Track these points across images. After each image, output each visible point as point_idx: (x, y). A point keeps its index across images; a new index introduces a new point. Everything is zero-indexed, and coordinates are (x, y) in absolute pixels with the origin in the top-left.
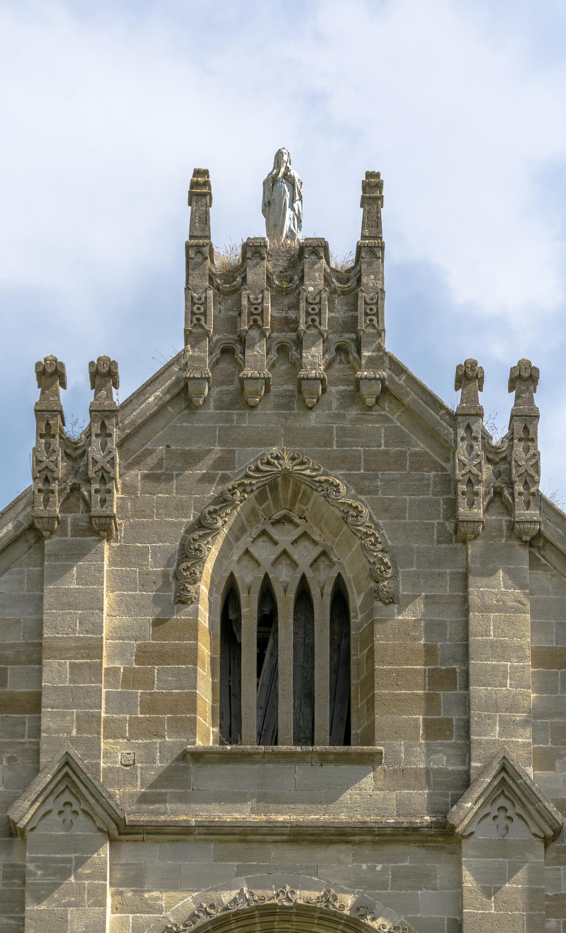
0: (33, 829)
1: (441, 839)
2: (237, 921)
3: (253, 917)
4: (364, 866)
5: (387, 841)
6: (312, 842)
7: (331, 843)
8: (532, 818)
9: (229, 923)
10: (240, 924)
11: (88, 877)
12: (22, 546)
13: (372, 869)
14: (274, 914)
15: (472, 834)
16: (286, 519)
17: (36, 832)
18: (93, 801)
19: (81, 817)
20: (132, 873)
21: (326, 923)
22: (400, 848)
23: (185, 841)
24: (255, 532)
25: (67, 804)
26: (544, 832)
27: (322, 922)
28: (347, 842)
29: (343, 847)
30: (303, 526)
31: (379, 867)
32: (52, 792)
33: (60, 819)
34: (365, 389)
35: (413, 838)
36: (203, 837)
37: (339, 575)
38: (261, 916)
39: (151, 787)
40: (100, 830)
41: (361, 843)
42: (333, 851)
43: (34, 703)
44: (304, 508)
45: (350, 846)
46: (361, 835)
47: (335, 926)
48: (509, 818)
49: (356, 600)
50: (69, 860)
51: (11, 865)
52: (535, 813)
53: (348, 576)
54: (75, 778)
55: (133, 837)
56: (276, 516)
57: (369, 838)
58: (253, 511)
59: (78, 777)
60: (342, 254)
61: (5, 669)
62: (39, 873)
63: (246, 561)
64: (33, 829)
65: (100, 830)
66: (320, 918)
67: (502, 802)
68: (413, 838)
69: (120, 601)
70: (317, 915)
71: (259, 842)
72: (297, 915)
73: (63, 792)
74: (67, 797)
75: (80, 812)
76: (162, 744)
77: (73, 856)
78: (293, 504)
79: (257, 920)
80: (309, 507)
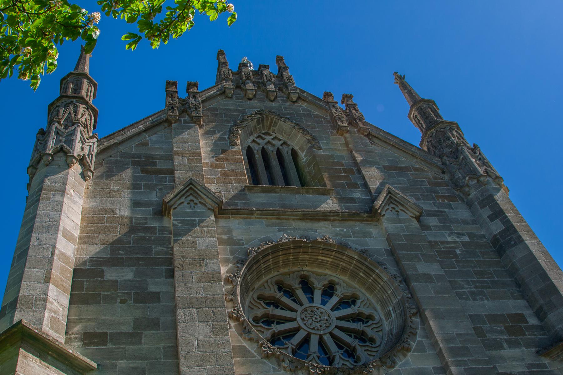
0: (175, 208)
1: (370, 219)
2: (283, 250)
3: (289, 249)
4: (338, 229)
5: (345, 220)
6: (311, 220)
7: (319, 220)
8: (408, 210)
9: (278, 251)
10: (284, 252)
11: (205, 227)
12: (161, 127)
13: (343, 230)
14: (300, 247)
15: (384, 215)
16: (267, 134)
17: (177, 210)
18: (204, 197)
19: (199, 205)
20: (226, 230)
21: (326, 252)
22: (352, 223)
23: (250, 218)
24: (256, 135)
25: (191, 201)
26: (415, 215)
27: (324, 252)
28: (327, 220)
29: (326, 222)
30: (274, 135)
31: (345, 230)
32: (183, 195)
33: (189, 206)
34: (292, 96)
35: (357, 218)
36: (259, 216)
37: (293, 149)
38: (295, 248)
39: (229, 199)
40: (209, 209)
41: (334, 220)
42: (322, 224)
43: (171, 172)
44: (275, 128)
45: (329, 222)
46: (333, 216)
47: (330, 253)
48: (397, 211)
49: (302, 155)
50: (195, 220)
51: (163, 227)
52: (408, 208)
53: (296, 148)
54: (195, 189)
55: (224, 215)
56: (264, 132)
57: (337, 218)
58: (255, 126)
59: (197, 189)
60: (274, 69)
61: (156, 162)
62: (180, 225)
63: (253, 143)
64: (175, 208)
65: (209, 209)
66: (323, 249)
67: (392, 205)
68: (357, 218)
69: (206, 144)
70: (322, 246)
71: (286, 219)
72: (312, 248)
73: (189, 196)
74: (191, 198)
75: (198, 203)
76: (232, 186)
77: (196, 219)
78: (269, 128)
79: (292, 251)
80: (277, 127)
